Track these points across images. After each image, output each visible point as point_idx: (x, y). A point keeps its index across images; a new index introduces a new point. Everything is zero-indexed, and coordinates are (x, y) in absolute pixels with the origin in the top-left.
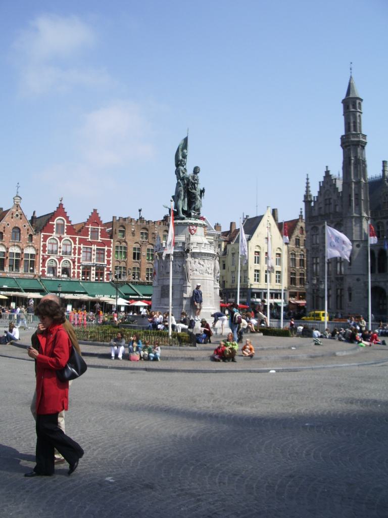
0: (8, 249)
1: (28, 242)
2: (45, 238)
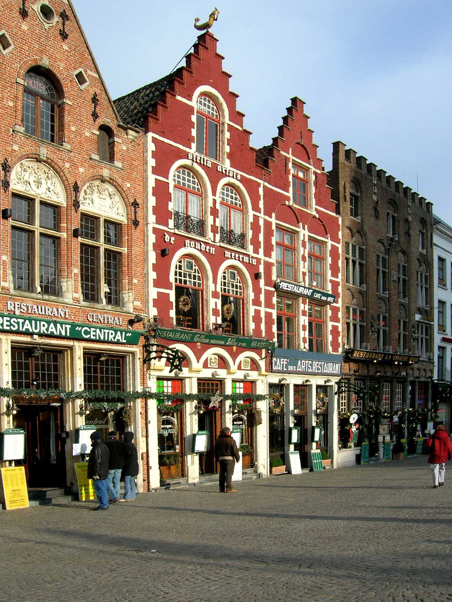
2: (165, 158)
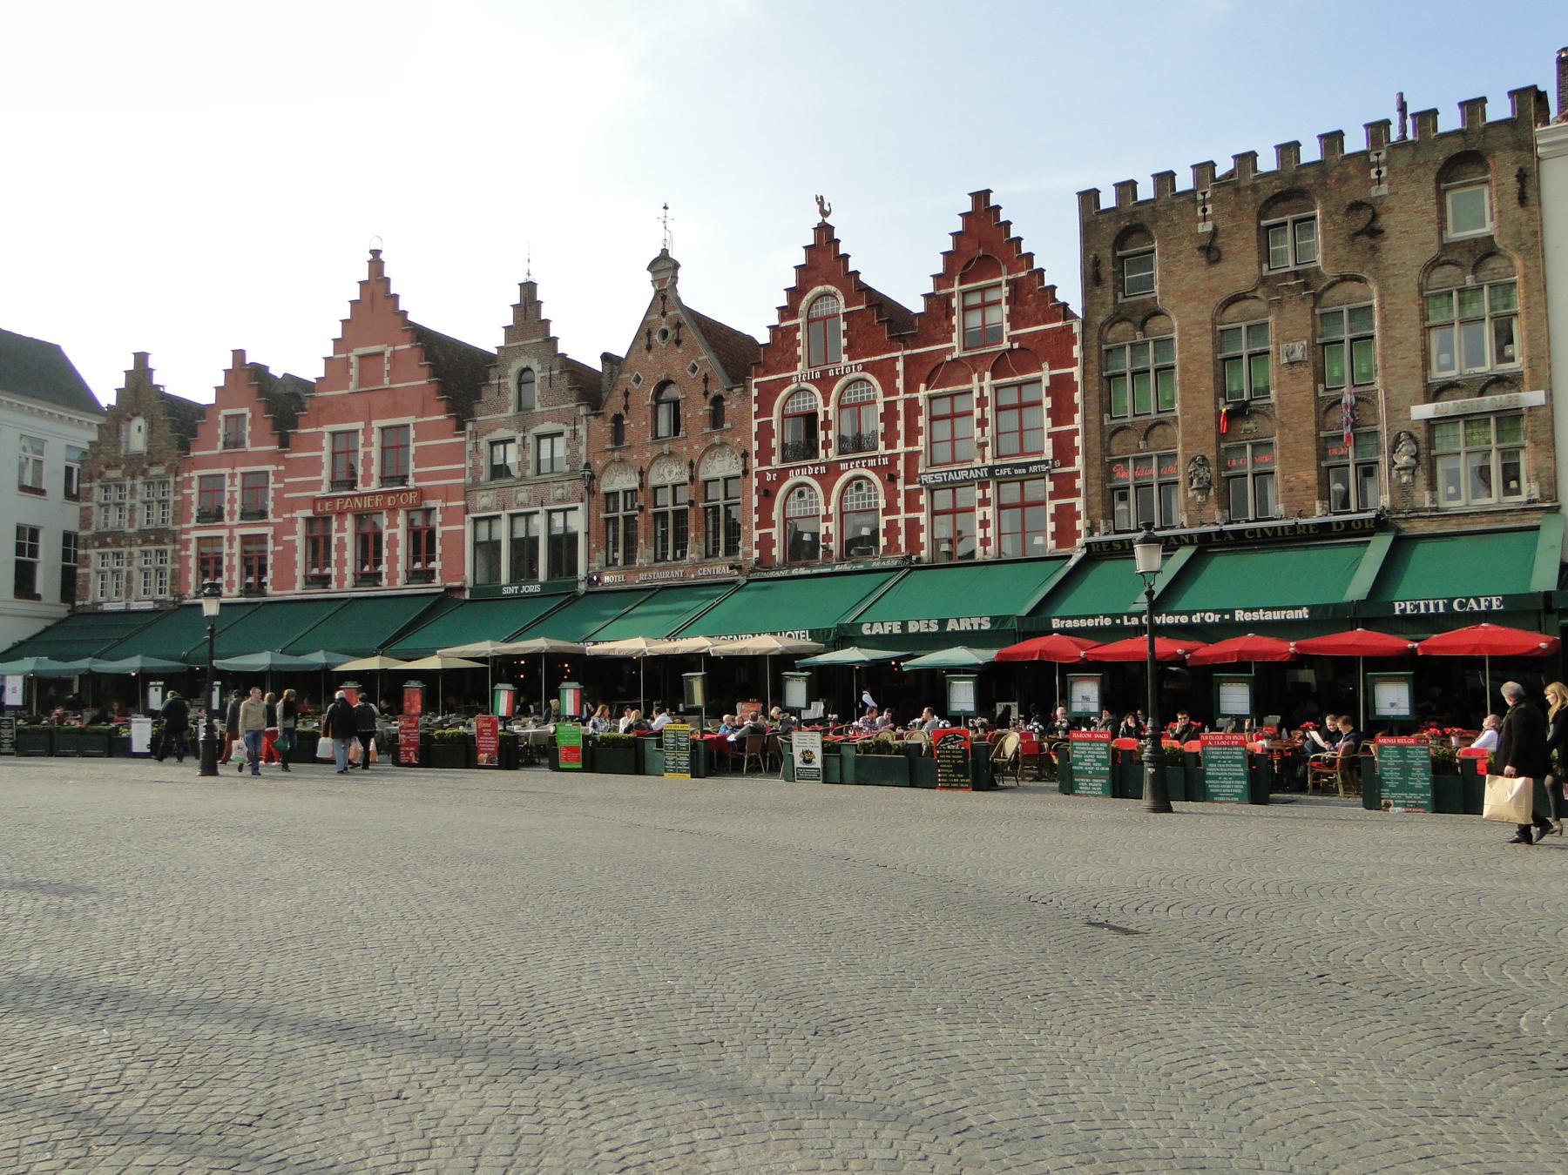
1: (707, 430)
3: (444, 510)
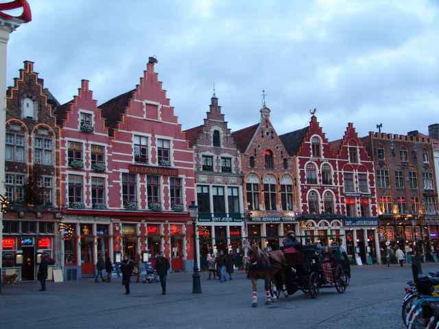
0: (262, 179)
3: (186, 180)
